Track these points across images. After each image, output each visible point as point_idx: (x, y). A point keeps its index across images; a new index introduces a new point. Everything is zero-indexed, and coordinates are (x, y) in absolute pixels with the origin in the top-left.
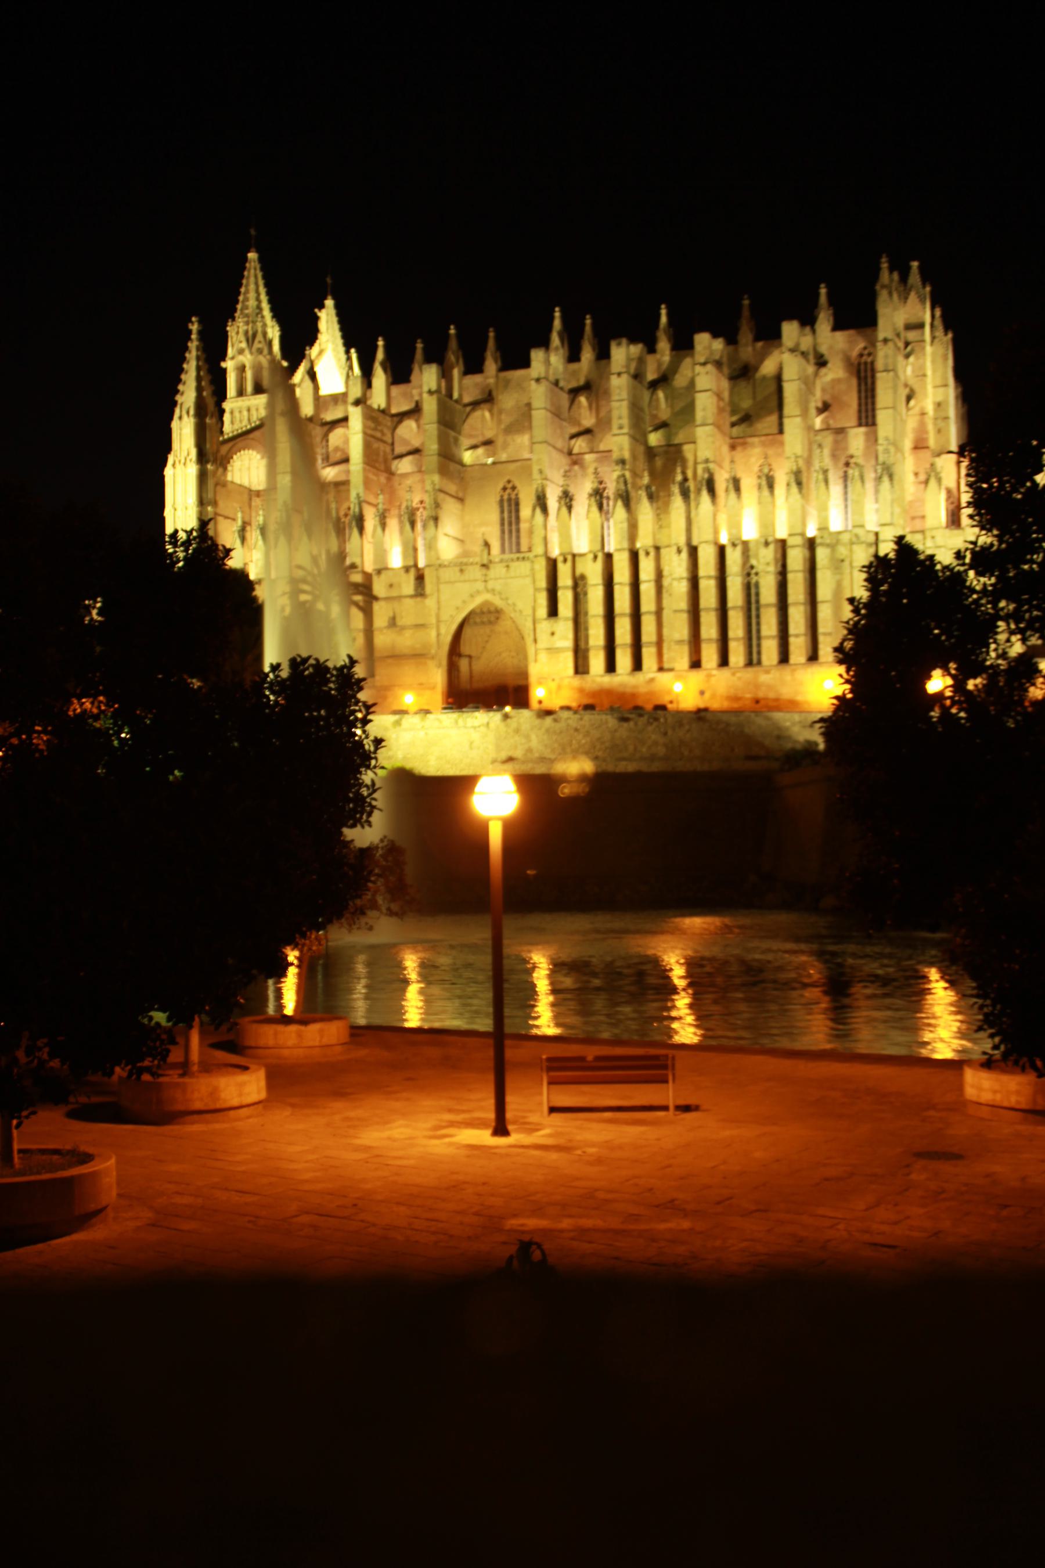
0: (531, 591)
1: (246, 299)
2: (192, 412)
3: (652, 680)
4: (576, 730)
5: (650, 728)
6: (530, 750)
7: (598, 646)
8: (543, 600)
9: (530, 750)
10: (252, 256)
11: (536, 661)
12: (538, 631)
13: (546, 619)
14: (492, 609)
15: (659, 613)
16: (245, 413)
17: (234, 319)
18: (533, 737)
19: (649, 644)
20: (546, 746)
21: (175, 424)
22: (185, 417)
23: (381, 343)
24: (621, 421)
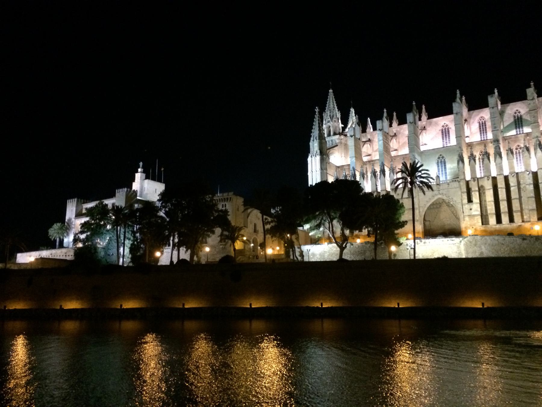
0: (460, 193)
1: (329, 105)
2: (317, 138)
3: (520, 226)
4: (503, 244)
5: (537, 243)
6: (482, 253)
7: (493, 213)
8: (465, 196)
9: (482, 253)
10: (331, 91)
11: (464, 220)
12: (464, 209)
13: (467, 204)
14: (438, 202)
15: (520, 198)
16: (331, 142)
17: (325, 112)
18: (483, 247)
19: (517, 211)
20: (489, 251)
21: (311, 144)
22: (315, 140)
23: (385, 111)
24: (495, 125)
